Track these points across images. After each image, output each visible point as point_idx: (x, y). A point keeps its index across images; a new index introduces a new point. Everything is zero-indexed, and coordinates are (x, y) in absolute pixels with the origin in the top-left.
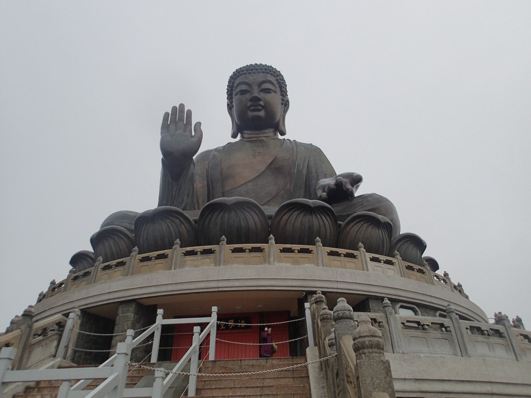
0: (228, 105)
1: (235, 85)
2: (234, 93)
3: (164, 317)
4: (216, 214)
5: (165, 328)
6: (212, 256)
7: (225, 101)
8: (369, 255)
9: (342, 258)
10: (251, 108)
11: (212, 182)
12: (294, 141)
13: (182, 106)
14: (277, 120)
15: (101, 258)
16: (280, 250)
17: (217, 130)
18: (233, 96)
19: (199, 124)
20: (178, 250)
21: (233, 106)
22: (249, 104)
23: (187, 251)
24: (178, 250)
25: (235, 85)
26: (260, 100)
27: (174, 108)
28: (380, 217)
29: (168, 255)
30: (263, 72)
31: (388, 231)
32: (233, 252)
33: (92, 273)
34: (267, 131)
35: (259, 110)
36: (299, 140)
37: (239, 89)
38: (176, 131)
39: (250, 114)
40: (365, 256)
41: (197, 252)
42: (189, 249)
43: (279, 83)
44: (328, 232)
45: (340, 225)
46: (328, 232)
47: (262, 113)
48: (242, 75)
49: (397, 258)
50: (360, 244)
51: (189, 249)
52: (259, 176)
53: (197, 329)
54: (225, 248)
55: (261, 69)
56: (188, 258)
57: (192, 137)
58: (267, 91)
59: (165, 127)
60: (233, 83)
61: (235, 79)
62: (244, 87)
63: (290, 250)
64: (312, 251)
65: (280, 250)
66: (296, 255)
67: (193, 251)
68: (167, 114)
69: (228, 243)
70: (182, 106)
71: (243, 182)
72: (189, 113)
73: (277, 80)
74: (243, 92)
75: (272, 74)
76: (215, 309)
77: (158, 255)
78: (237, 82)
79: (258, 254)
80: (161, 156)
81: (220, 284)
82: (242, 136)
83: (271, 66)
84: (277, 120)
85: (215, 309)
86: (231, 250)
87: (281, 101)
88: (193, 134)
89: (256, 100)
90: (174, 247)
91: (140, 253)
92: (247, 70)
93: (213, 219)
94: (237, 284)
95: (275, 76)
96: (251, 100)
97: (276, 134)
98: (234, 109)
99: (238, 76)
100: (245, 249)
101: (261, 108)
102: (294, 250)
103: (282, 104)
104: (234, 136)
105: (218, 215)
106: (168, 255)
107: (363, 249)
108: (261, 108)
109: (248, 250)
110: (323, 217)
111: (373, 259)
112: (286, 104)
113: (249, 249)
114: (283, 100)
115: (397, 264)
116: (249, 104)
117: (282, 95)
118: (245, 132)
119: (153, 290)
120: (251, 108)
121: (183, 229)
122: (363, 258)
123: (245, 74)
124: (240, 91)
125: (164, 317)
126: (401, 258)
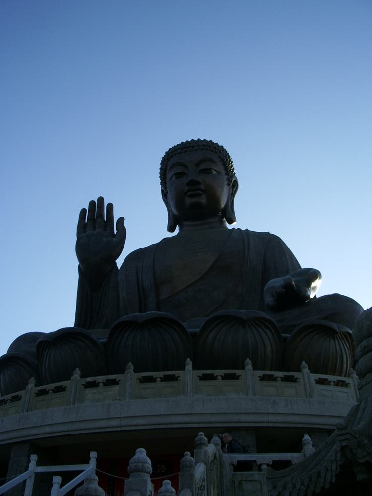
0: (162, 192)
1: (168, 167)
2: (168, 176)
3: (39, 463)
5: (37, 475)
6: (116, 388)
7: (159, 187)
8: (314, 377)
9: (279, 383)
10: (189, 194)
12: (247, 230)
13: (101, 200)
14: (223, 205)
16: (199, 377)
17: (147, 223)
18: (167, 180)
19: (121, 220)
21: (167, 193)
22: (186, 188)
23: (88, 383)
25: (168, 167)
26: (199, 183)
27: (92, 204)
28: (335, 326)
29: (66, 387)
30: (202, 150)
31: (348, 342)
32: (141, 382)
34: (211, 220)
35: (200, 195)
36: (251, 229)
37: (172, 172)
38: (95, 230)
39: (188, 201)
40: (309, 378)
41: (99, 383)
42: (89, 379)
43: (222, 160)
44: (269, 349)
45: (285, 339)
46: (269, 349)
47: (203, 200)
48: (175, 155)
49: (352, 378)
50: (303, 363)
51: (89, 379)
53: (57, 480)
54: (130, 377)
55: (199, 146)
56: (88, 391)
57: (114, 236)
58: (207, 171)
59: (82, 227)
60: (166, 165)
61: (168, 160)
62: (179, 169)
63: (212, 378)
64: (239, 376)
65: (199, 377)
66: (219, 382)
67: (95, 382)
68: (83, 211)
69: (136, 371)
70: (101, 200)
72: (110, 206)
73: (220, 157)
74: (178, 175)
75: (212, 151)
76: (93, 455)
77: (56, 388)
78: (170, 163)
80: (78, 263)
81: (123, 422)
82: (180, 229)
83: (211, 141)
84: (223, 205)
85: (93, 455)
86: (139, 379)
87: (226, 182)
88: (115, 232)
89: (193, 183)
90: (72, 378)
91: (36, 386)
92: (182, 149)
94: (142, 421)
95: (216, 153)
96: (188, 184)
97: (222, 223)
98: (169, 196)
99: (171, 157)
100: (156, 378)
101: (201, 192)
102: (217, 376)
103: (228, 185)
104: (171, 229)
106: (66, 387)
107: (306, 370)
108: (201, 192)
109: (158, 380)
110: (261, 331)
111: (321, 382)
112: (234, 186)
113: (161, 378)
114: (228, 180)
115: (352, 385)
116: (186, 188)
117: (227, 174)
118: (185, 223)
119: (47, 429)
120: (189, 194)
122: (306, 380)
123: (180, 153)
124: (175, 174)
125: (39, 463)
126: (357, 377)
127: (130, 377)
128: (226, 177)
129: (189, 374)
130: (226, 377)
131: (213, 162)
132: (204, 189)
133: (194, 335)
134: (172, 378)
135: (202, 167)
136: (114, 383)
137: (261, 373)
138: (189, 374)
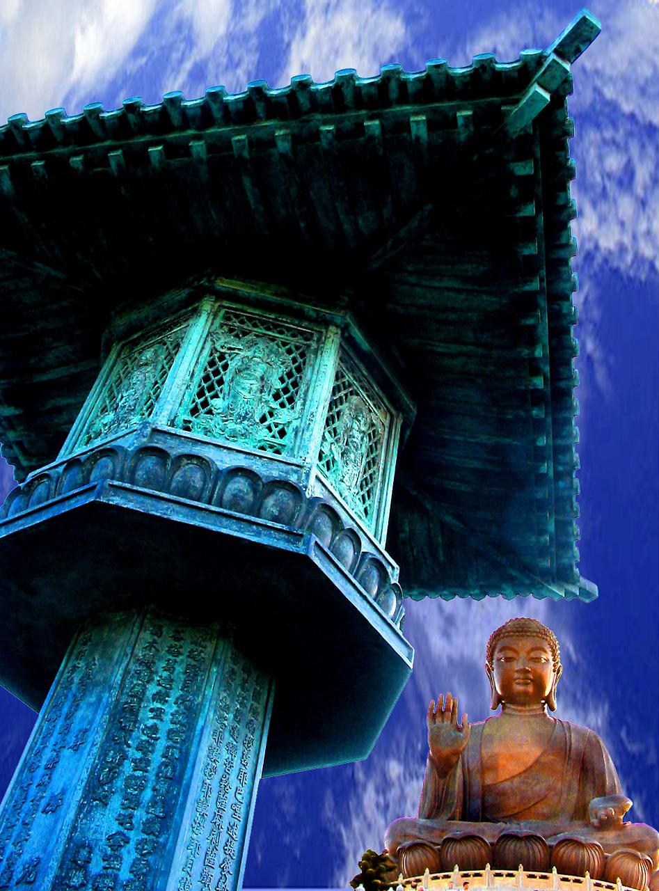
4: (509, 843)
11: (468, 769)
15: (427, 870)
20: (487, 871)
24: (487, 871)
33: (423, 881)
35: (527, 684)
52: (524, 771)
54: (521, 873)
56: (497, 878)
58: (537, 660)
69: (524, 870)
71: (507, 777)
79: (545, 880)
84: (547, 693)
93: (507, 847)
103: (554, 671)
105: (511, 843)
121: (483, 852)
127: (521, 873)
128: (553, 663)
129: (554, 875)
130: (575, 881)
131: (545, 652)
132: (532, 678)
133: (551, 847)
134: (545, 877)
135: (533, 655)
136: (511, 875)
137: (595, 881)
138: (554, 875)
